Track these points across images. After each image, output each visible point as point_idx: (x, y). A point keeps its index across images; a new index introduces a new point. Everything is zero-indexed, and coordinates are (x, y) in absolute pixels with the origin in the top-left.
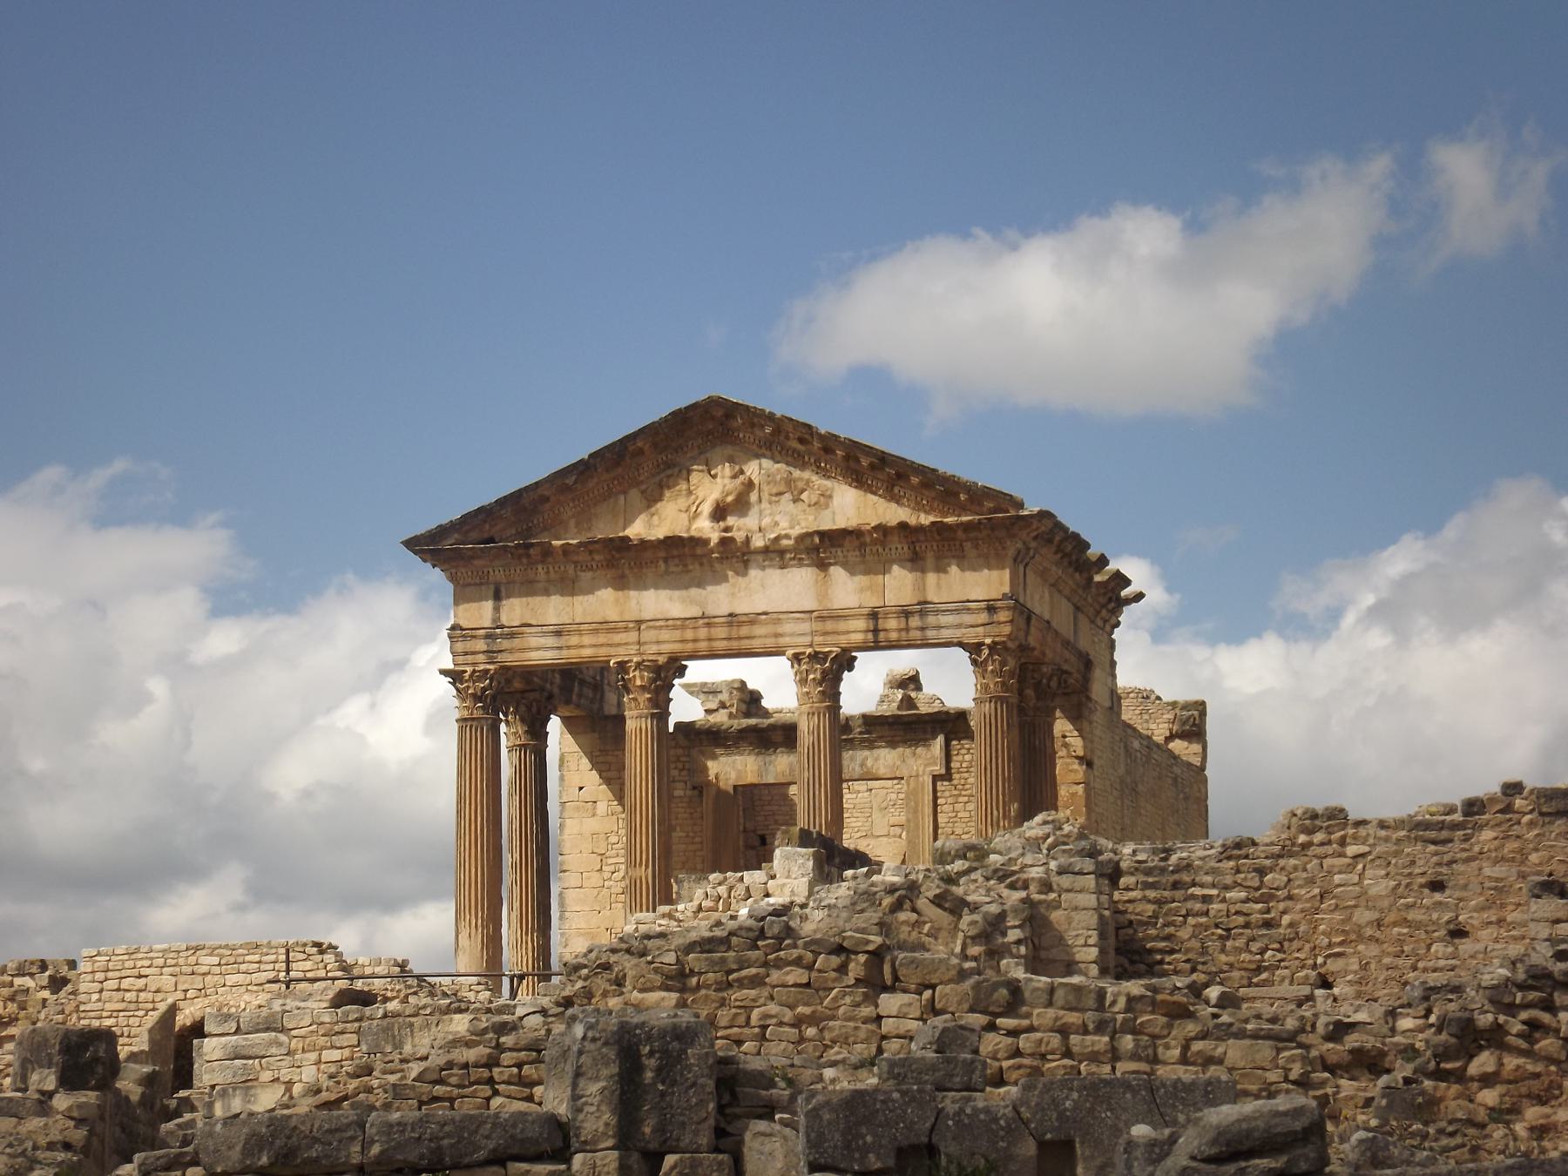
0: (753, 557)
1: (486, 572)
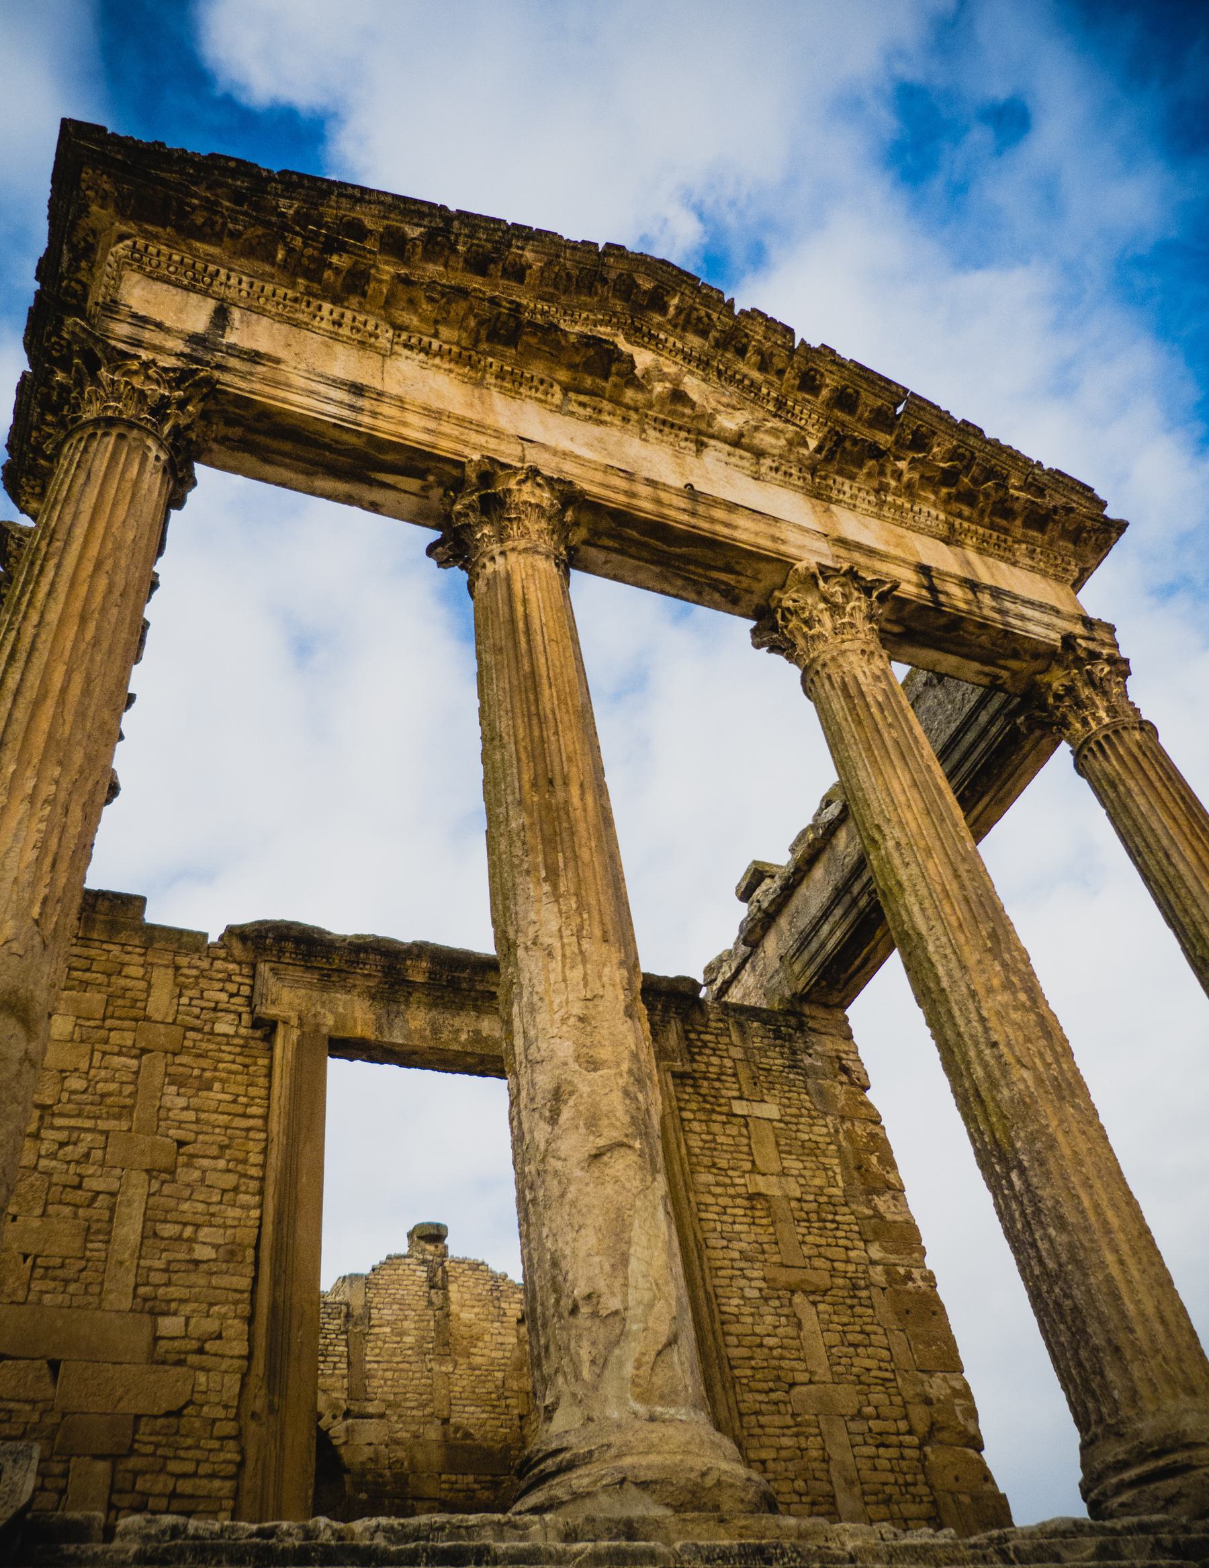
0: (712, 442)
1: (212, 268)
